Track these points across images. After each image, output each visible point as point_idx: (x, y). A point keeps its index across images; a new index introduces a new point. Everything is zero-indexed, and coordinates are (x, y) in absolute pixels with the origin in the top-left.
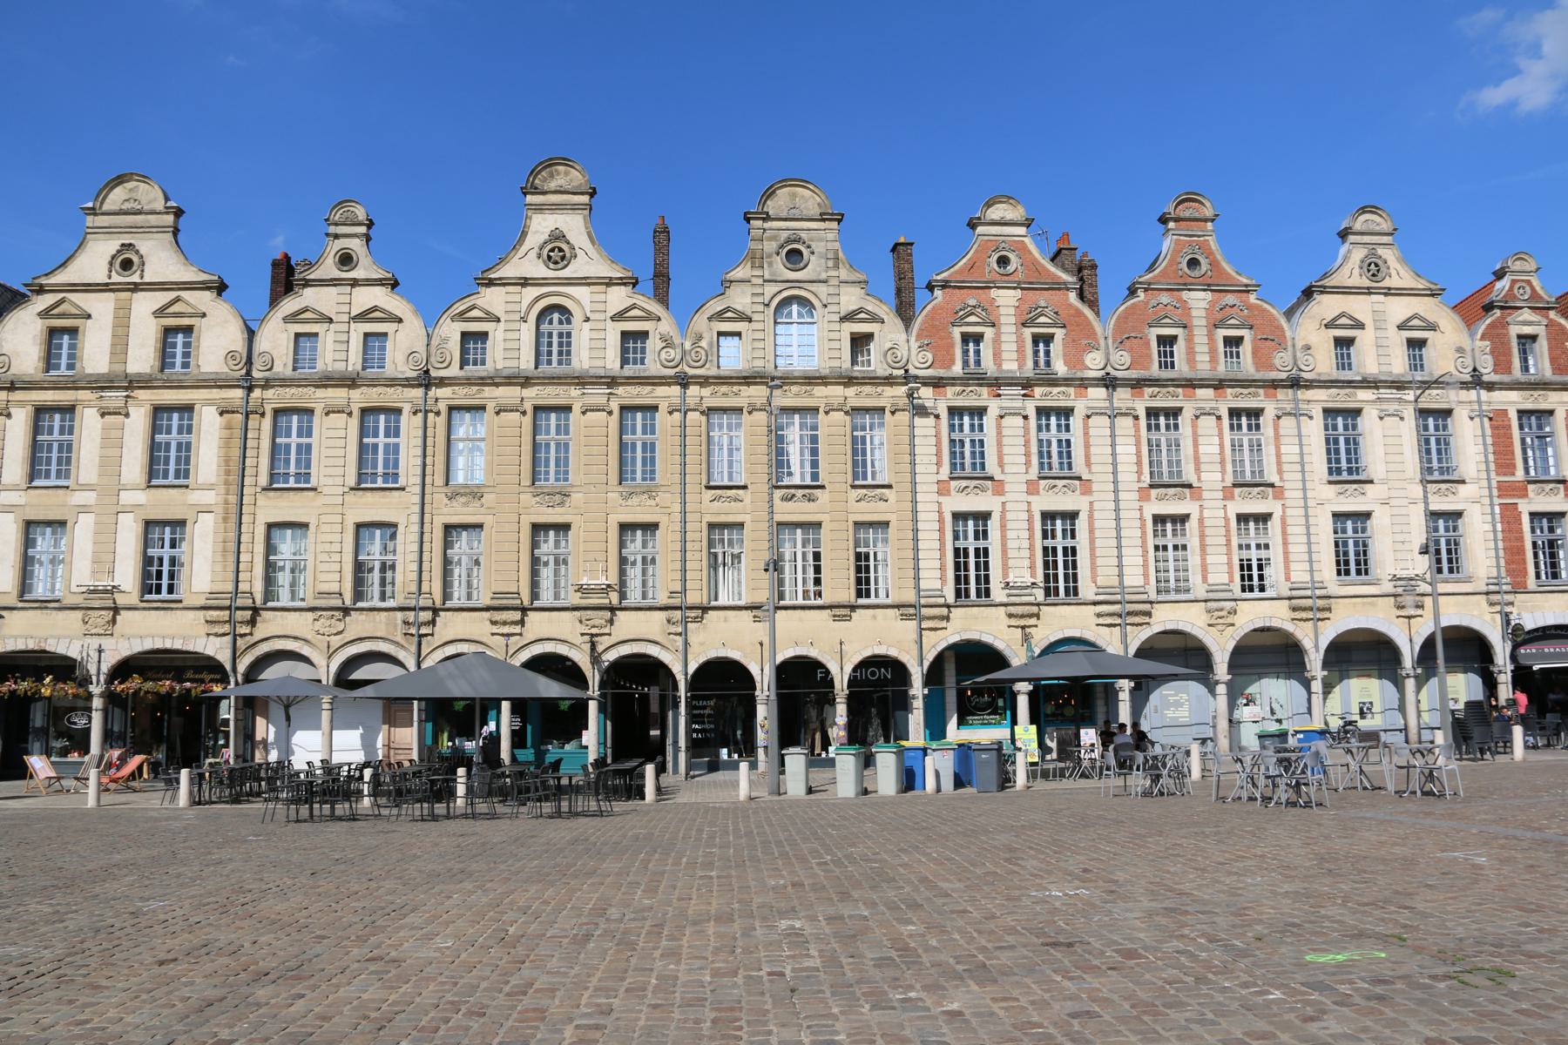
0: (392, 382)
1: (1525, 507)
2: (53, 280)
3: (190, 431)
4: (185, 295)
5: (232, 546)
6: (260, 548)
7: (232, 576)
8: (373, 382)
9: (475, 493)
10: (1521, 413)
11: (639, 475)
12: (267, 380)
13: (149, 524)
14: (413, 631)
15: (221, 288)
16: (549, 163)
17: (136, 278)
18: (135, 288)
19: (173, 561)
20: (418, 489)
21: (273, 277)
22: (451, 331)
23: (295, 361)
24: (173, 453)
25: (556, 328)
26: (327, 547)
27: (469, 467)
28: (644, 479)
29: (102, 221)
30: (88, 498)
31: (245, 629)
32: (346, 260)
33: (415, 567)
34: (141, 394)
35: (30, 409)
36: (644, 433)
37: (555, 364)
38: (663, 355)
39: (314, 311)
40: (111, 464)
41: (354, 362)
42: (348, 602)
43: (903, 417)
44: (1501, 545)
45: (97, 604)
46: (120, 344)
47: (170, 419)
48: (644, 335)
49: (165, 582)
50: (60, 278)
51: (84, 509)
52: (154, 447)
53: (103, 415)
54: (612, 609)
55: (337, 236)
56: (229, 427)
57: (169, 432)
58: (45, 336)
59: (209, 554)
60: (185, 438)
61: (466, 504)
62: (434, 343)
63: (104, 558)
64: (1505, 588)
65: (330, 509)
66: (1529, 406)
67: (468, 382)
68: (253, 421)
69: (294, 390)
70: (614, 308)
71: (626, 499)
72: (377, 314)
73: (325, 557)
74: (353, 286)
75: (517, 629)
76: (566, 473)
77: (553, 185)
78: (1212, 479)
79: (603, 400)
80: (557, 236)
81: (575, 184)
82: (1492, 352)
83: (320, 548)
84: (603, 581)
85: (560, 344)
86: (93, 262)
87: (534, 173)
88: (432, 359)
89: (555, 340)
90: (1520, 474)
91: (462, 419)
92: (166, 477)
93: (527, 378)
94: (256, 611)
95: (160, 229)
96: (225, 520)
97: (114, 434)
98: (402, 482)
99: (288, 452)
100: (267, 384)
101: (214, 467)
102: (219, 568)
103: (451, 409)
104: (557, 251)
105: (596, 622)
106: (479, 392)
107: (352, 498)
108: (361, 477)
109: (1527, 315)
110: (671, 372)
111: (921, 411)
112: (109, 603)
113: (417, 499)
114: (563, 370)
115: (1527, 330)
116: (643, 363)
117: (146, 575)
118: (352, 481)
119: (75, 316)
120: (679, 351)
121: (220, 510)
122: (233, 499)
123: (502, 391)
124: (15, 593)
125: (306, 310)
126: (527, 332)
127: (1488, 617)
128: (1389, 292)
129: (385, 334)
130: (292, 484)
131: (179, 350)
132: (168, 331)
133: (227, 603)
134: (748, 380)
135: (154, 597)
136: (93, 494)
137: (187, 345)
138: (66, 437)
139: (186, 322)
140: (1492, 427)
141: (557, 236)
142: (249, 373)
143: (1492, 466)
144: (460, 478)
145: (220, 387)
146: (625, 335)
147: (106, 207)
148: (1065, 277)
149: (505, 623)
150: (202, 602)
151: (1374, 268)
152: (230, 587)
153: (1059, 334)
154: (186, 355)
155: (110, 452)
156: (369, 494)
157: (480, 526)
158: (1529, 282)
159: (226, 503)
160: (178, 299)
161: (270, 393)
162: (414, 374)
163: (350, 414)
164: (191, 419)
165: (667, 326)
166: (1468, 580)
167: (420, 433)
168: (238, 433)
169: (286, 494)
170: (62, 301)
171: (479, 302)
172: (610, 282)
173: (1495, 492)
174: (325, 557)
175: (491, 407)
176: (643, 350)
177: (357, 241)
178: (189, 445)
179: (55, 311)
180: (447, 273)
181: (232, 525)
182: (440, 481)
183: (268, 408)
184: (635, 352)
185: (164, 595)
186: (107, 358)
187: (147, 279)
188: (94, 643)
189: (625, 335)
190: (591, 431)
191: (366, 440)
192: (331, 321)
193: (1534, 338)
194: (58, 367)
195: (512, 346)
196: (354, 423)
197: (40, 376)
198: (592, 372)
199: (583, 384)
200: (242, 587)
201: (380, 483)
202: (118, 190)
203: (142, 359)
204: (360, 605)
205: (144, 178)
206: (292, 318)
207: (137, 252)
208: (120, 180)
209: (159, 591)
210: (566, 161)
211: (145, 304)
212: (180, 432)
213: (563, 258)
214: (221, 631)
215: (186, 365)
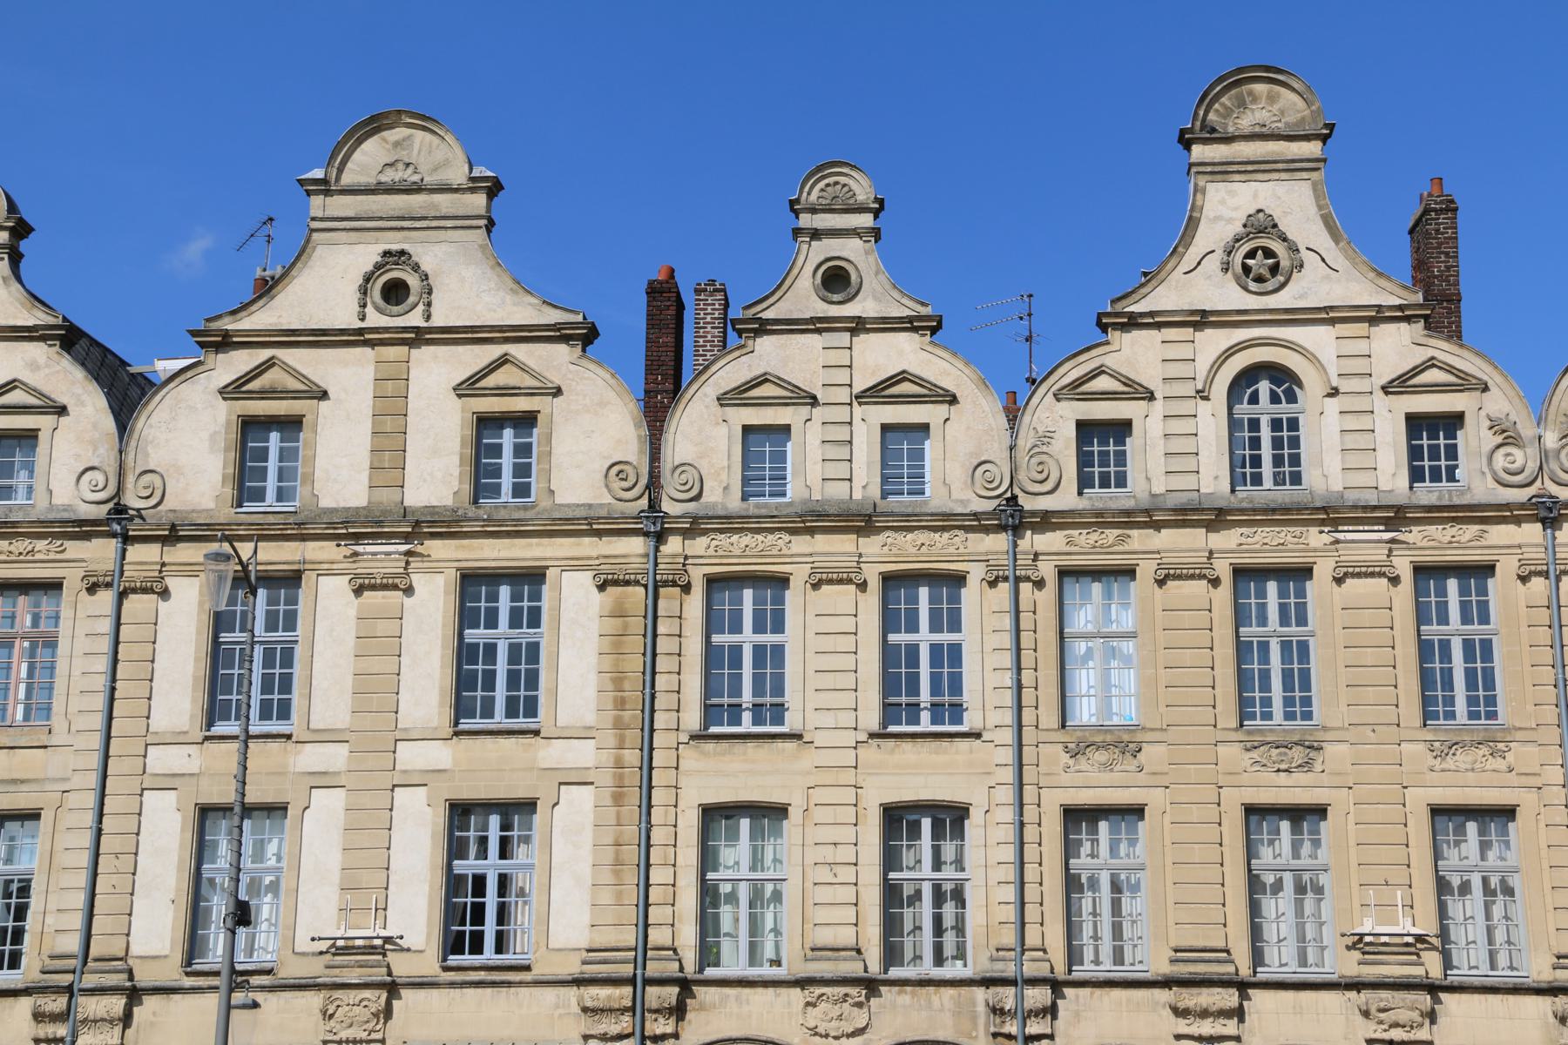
0: (946, 522)
2: (247, 323)
3: (535, 621)
4: (518, 351)
5: (632, 853)
6: (689, 856)
7: (631, 914)
8: (908, 522)
9: (1123, 743)
11: (1461, 706)
12: (695, 519)
13: (461, 812)
14: (1012, 1028)
15: (586, 337)
16: (1237, 79)
17: (415, 319)
18: (418, 337)
19: (504, 882)
20: (1008, 736)
21: (650, 316)
22: (1054, 420)
23: (745, 481)
24: (502, 667)
25: (1265, 410)
26: (828, 854)
27: (1107, 691)
28: (1473, 715)
29: (340, 205)
30: (334, 757)
31: (662, 1026)
32: (836, 280)
33: (1010, 893)
35: (452, 575)
36: (1284, 621)
37: (1268, 482)
38: (1500, 461)
39: (780, 382)
40: (377, 687)
41: (865, 483)
42: (875, 968)
45: (353, 976)
46: (389, 451)
47: (493, 597)
48: (1454, 421)
49: (490, 928)
50: (262, 318)
51: (322, 781)
52: (465, 653)
53: (358, 592)
54: (1433, 989)
55: (816, 234)
56: (619, 613)
57: (492, 622)
58: (234, 435)
59: (585, 869)
60: (525, 634)
61: (1108, 766)
62: (1025, 441)
63: (366, 883)
65: (831, 768)
67: (1100, 520)
68: (669, 600)
69: (747, 539)
70: (1387, 369)
71: (1442, 756)
72: (906, 388)
73: (824, 875)
74: (854, 332)
75: (1230, 1027)
76: (1307, 701)
77: (1246, 122)
79: (1380, 554)
80: (1261, 225)
81: (1291, 118)
83: (814, 854)
84: (1405, 926)
85: (1277, 443)
86: (328, 286)
87: (1207, 99)
88: (1022, 476)
89: (1266, 434)
91: (1086, 596)
92: (488, 712)
93: (1221, 512)
94: (685, 986)
95: (461, 221)
96: (618, 799)
97: (383, 627)
98: (970, 721)
99: (736, 662)
100: (694, 527)
101: (591, 692)
102: (606, 897)
103: (1064, 573)
104: (1262, 256)
105: (1403, 1016)
106: (1121, 539)
107: (871, 753)
108: (890, 712)
110: (1522, 495)
112: (379, 975)
113: (1007, 755)
114: (1286, 494)
116: (1451, 478)
117: (452, 913)
118: (871, 718)
119: (295, 395)
120: (1533, 451)
121: (606, 778)
122: (632, 757)
123: (1167, 538)
124: (178, 957)
125: (763, 380)
126: (1211, 421)
129: (925, 428)
130: (747, 725)
131: (507, 461)
132: (486, 423)
133: (627, 970)
135: (467, 959)
136: (343, 750)
137: (523, 450)
138: (279, 635)
139: (521, 404)
141: (1261, 225)
142: (654, 505)
144: (1085, 712)
145: (599, 534)
146: (1416, 423)
147: (347, 179)
149: (1204, 1014)
150: (573, 967)
152: (629, 937)
154: (522, 471)
155: (375, 665)
156: (907, 746)
157: (1138, 811)
159: (619, 764)
160: (503, 361)
161: (699, 545)
162: (989, 506)
163: (863, 586)
164: (536, 596)
165: (1501, 401)
167: (1007, 622)
168: (637, 624)
169: (739, 747)
170: (269, 364)
171: (1110, 361)
172: (1377, 316)
174: (824, 875)
175: (1147, 570)
176: (1452, 452)
177: (856, 243)
178: (534, 649)
179: (254, 385)
180: (1047, 304)
181: (631, 810)
182: (1050, 718)
183: (697, 576)
184: (1434, 456)
185: (489, 954)
186: (364, 477)
187: (438, 321)
189: (1416, 423)
190: (1357, 619)
191: (717, 639)
192: (814, 401)
194: (259, 495)
195: (1178, 448)
196: (871, 604)
197: (226, 513)
198: (1351, 497)
199: (1335, 523)
200: (657, 936)
201: (925, 724)
202: (370, 145)
203: (435, 478)
204: (895, 973)
205: (425, 121)
206: (735, 397)
207: (416, 268)
208: (374, 125)
209: (477, 948)
210: (1271, 73)
211: (435, 373)
212: (515, 622)
213: (1274, 269)
214: (614, 1029)
215: (521, 490)
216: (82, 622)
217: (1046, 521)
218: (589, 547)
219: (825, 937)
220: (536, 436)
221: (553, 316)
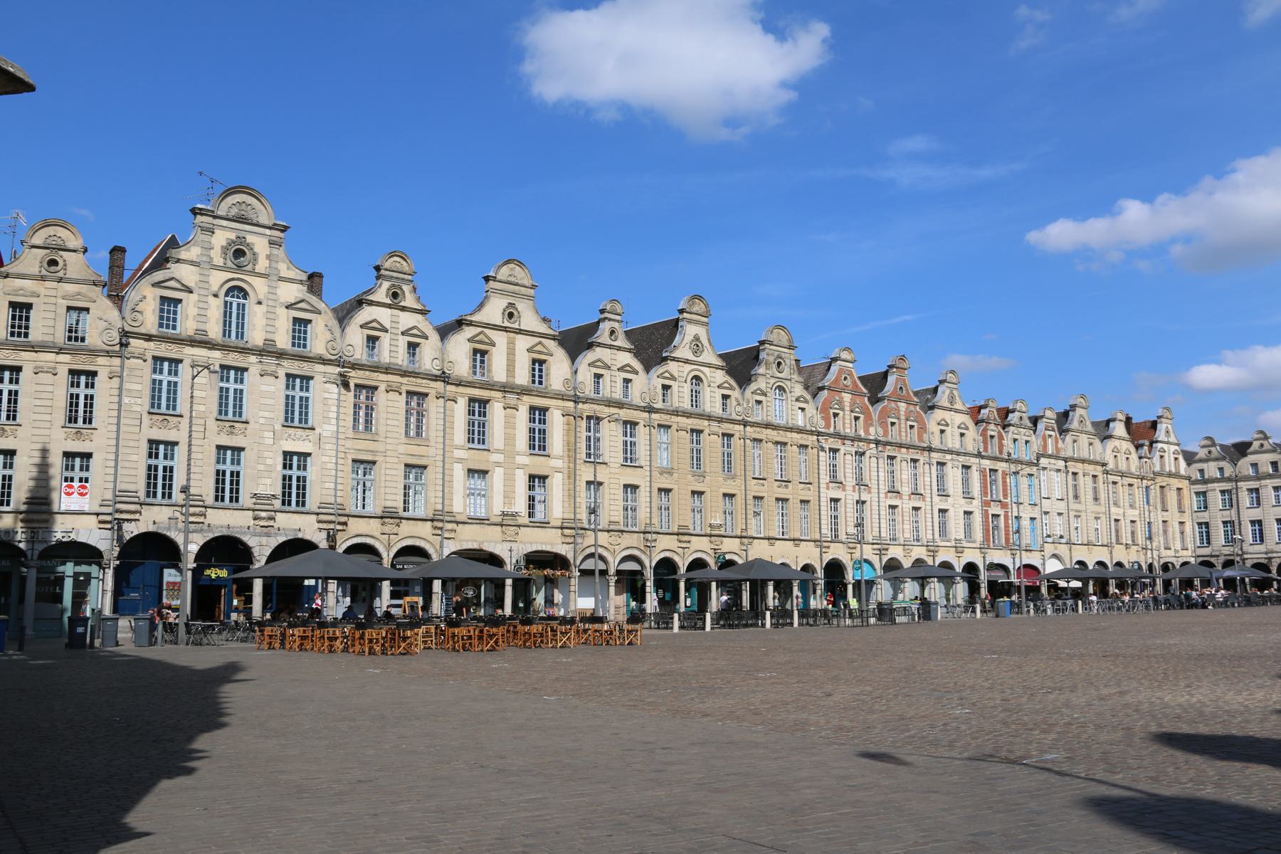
1: (991, 512)
34: (525, 398)
40: (510, 439)
43: (815, 451)
51: (498, 464)
69: (596, 407)
78: (906, 490)
86: (493, 311)
104: (697, 346)
109: (992, 427)
111: (823, 449)
125: (599, 360)
128: (957, 411)
134: (768, 426)
141: (697, 338)
148: (865, 390)
151: (952, 400)
153: (862, 417)
161: (586, 406)
166: (974, 542)
175: (675, 427)
188: (507, 545)
203: (522, 377)
216: (433, 407)
217: (657, 411)
218: (560, 403)
219: (613, 519)
220: (544, 367)
221: (551, 332)
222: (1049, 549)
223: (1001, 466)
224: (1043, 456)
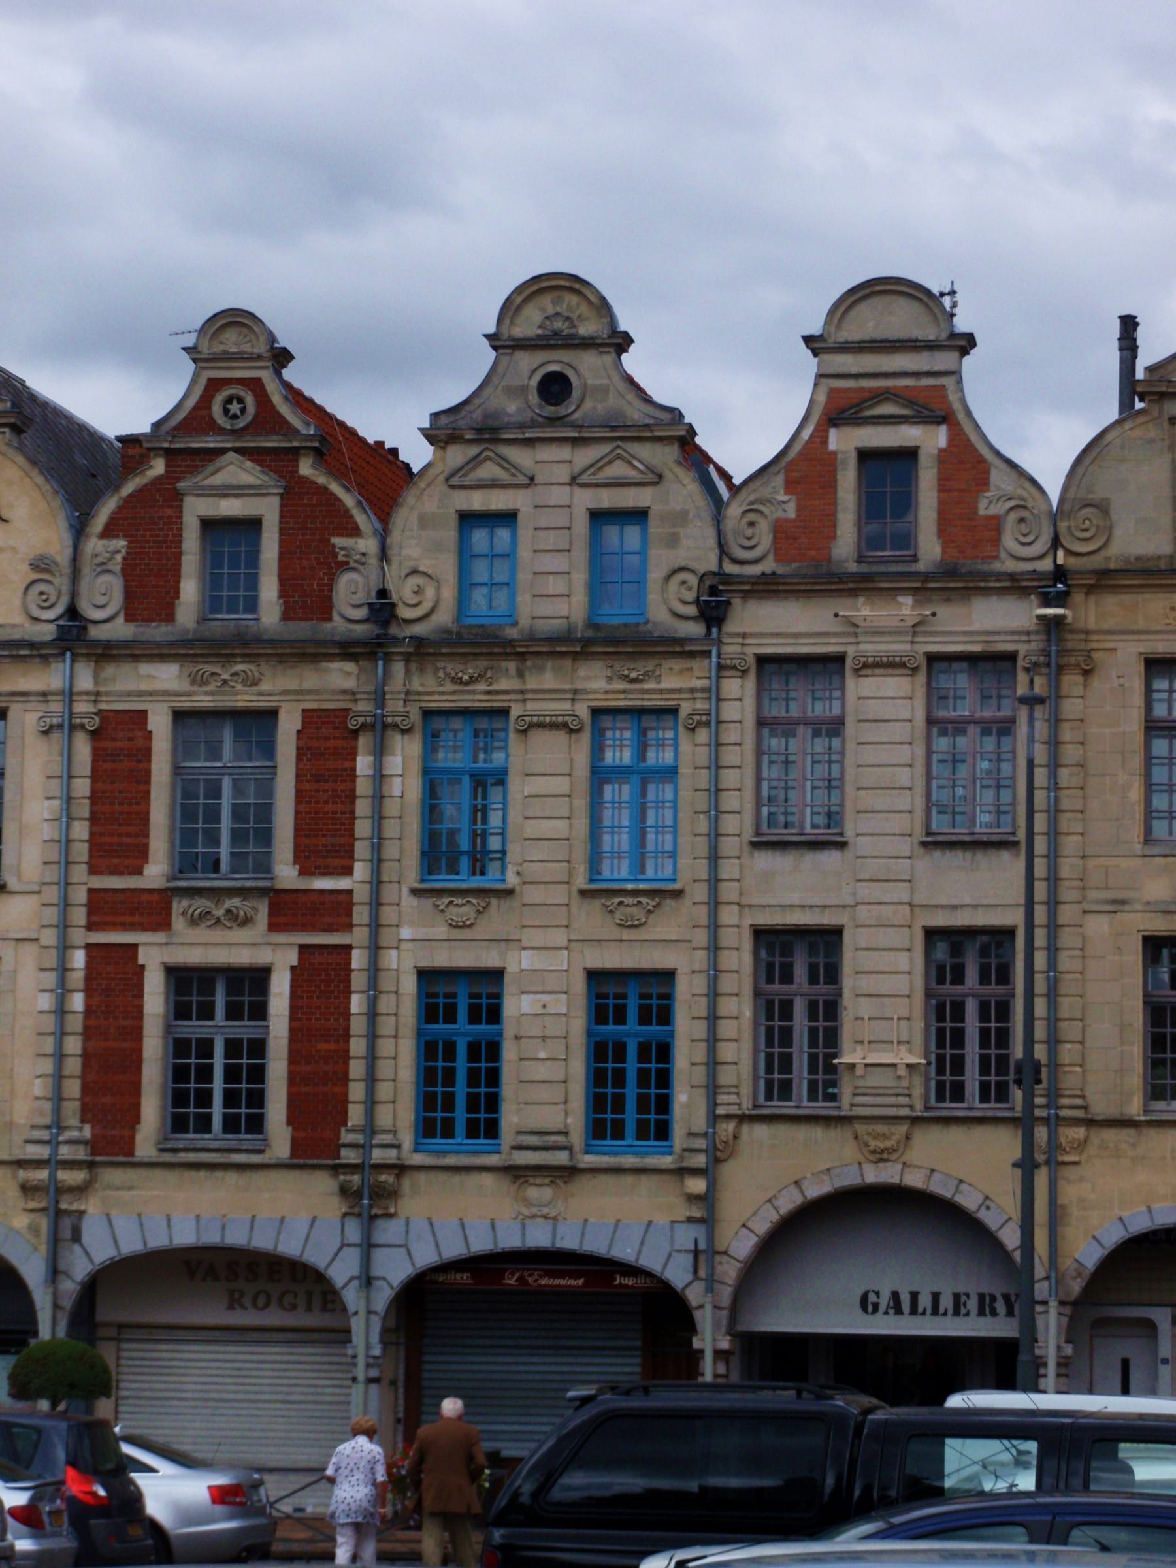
1: (154, 954)
10: (180, 716)
44: (73, 1045)
64: (65, 1152)
66: (203, 700)
82: (128, 570)
90: (156, 871)
109: (236, 471)
115: (230, 508)
127: (21, 1221)
140: (98, 756)
143: (81, 851)
158: (255, 385)
173: (79, 916)
193: (253, 524)
222: (777, 1171)
223: (290, 694)
224: (767, 587)
